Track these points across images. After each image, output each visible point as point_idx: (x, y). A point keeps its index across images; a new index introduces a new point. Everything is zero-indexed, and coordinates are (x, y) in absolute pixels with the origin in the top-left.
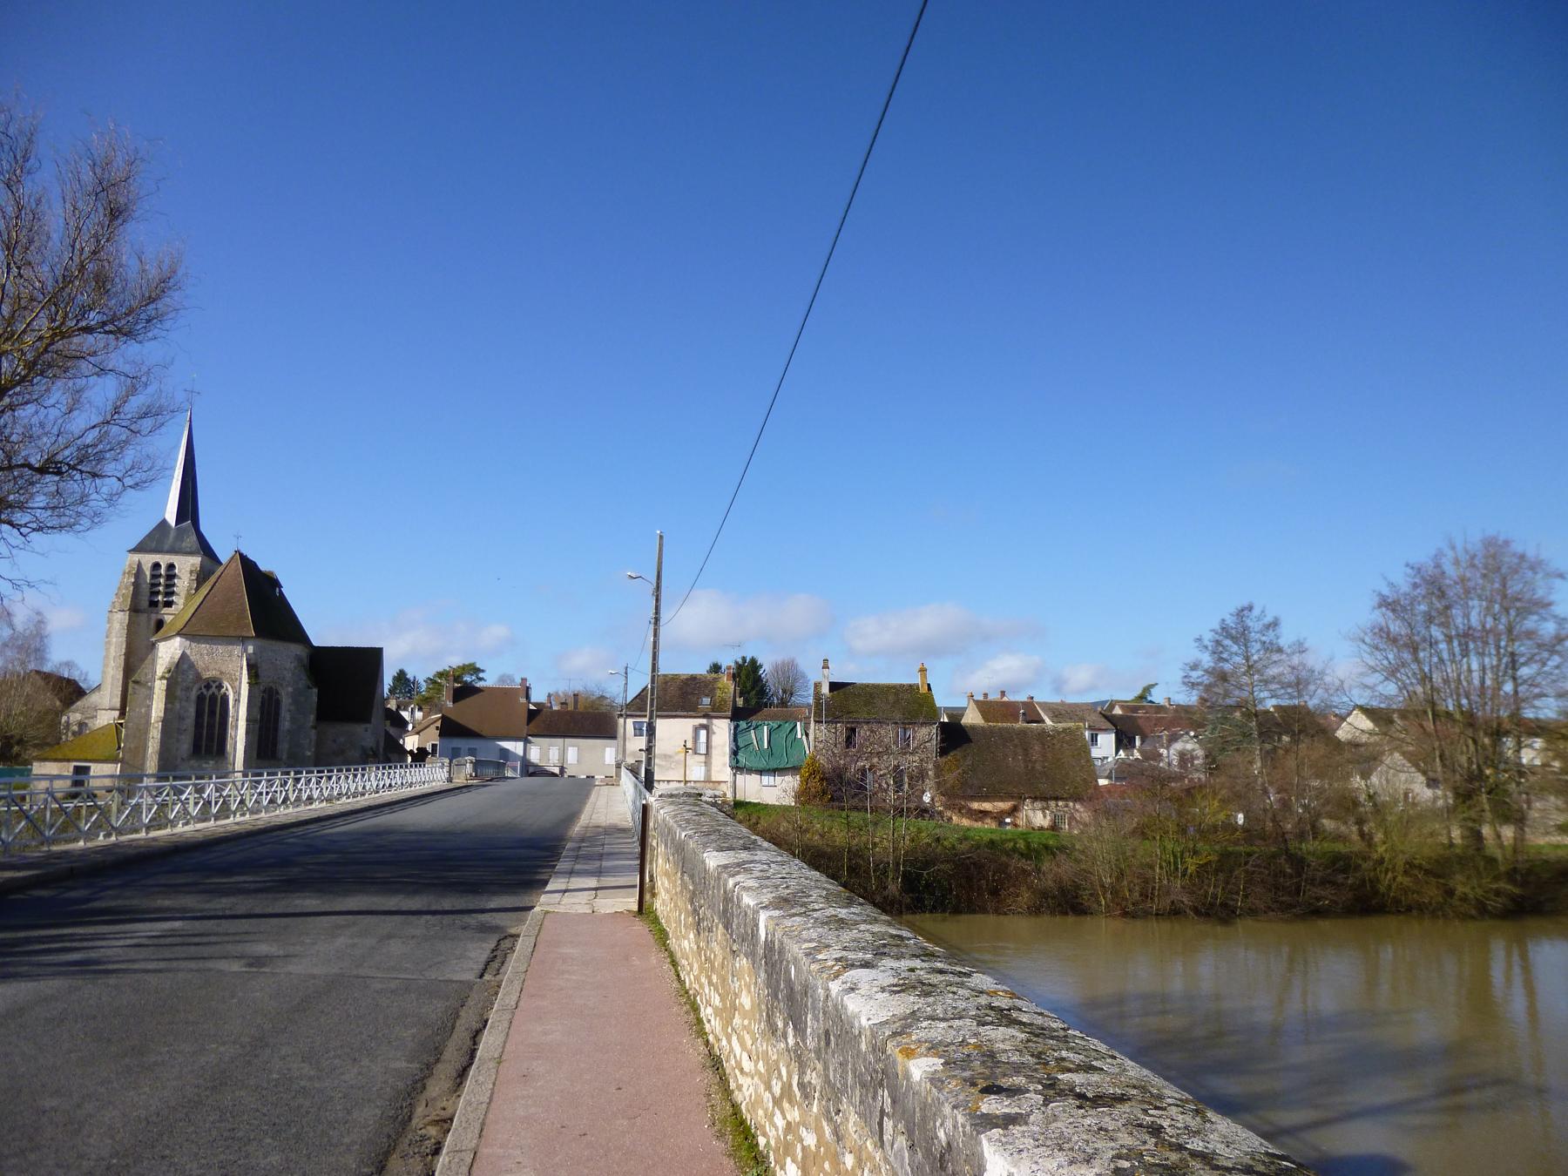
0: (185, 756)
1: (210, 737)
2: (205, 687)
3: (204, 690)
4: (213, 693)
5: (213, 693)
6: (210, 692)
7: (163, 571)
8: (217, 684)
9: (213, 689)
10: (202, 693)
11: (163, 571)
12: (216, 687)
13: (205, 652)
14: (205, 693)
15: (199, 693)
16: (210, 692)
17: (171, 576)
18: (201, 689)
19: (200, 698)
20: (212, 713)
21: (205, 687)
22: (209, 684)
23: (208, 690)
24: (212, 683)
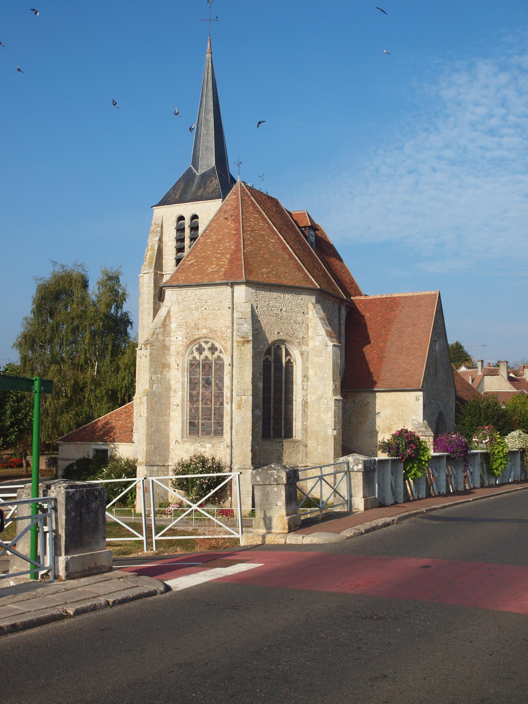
0: (179, 439)
1: (207, 415)
2: (197, 349)
3: (196, 354)
4: (206, 357)
5: (206, 357)
6: (203, 357)
7: (187, 223)
8: (209, 345)
9: (207, 353)
10: (194, 358)
11: (187, 223)
12: (209, 349)
13: (193, 306)
14: (198, 358)
15: (191, 357)
16: (215, 356)
17: (194, 228)
18: (192, 353)
19: (193, 365)
20: (208, 382)
21: (197, 349)
22: (200, 345)
23: (201, 354)
24: (204, 345)
